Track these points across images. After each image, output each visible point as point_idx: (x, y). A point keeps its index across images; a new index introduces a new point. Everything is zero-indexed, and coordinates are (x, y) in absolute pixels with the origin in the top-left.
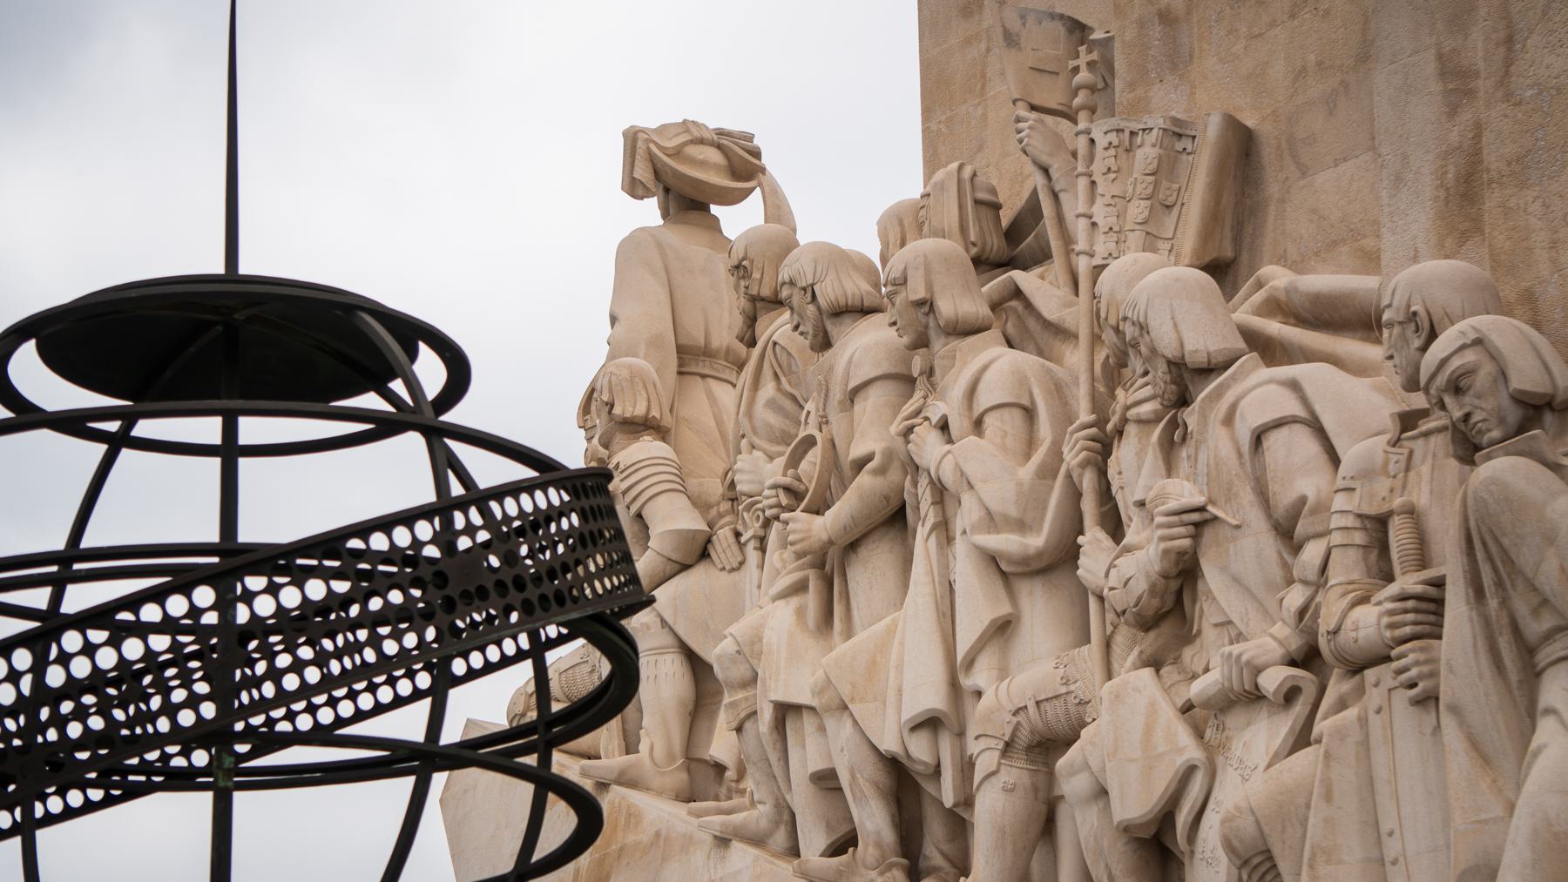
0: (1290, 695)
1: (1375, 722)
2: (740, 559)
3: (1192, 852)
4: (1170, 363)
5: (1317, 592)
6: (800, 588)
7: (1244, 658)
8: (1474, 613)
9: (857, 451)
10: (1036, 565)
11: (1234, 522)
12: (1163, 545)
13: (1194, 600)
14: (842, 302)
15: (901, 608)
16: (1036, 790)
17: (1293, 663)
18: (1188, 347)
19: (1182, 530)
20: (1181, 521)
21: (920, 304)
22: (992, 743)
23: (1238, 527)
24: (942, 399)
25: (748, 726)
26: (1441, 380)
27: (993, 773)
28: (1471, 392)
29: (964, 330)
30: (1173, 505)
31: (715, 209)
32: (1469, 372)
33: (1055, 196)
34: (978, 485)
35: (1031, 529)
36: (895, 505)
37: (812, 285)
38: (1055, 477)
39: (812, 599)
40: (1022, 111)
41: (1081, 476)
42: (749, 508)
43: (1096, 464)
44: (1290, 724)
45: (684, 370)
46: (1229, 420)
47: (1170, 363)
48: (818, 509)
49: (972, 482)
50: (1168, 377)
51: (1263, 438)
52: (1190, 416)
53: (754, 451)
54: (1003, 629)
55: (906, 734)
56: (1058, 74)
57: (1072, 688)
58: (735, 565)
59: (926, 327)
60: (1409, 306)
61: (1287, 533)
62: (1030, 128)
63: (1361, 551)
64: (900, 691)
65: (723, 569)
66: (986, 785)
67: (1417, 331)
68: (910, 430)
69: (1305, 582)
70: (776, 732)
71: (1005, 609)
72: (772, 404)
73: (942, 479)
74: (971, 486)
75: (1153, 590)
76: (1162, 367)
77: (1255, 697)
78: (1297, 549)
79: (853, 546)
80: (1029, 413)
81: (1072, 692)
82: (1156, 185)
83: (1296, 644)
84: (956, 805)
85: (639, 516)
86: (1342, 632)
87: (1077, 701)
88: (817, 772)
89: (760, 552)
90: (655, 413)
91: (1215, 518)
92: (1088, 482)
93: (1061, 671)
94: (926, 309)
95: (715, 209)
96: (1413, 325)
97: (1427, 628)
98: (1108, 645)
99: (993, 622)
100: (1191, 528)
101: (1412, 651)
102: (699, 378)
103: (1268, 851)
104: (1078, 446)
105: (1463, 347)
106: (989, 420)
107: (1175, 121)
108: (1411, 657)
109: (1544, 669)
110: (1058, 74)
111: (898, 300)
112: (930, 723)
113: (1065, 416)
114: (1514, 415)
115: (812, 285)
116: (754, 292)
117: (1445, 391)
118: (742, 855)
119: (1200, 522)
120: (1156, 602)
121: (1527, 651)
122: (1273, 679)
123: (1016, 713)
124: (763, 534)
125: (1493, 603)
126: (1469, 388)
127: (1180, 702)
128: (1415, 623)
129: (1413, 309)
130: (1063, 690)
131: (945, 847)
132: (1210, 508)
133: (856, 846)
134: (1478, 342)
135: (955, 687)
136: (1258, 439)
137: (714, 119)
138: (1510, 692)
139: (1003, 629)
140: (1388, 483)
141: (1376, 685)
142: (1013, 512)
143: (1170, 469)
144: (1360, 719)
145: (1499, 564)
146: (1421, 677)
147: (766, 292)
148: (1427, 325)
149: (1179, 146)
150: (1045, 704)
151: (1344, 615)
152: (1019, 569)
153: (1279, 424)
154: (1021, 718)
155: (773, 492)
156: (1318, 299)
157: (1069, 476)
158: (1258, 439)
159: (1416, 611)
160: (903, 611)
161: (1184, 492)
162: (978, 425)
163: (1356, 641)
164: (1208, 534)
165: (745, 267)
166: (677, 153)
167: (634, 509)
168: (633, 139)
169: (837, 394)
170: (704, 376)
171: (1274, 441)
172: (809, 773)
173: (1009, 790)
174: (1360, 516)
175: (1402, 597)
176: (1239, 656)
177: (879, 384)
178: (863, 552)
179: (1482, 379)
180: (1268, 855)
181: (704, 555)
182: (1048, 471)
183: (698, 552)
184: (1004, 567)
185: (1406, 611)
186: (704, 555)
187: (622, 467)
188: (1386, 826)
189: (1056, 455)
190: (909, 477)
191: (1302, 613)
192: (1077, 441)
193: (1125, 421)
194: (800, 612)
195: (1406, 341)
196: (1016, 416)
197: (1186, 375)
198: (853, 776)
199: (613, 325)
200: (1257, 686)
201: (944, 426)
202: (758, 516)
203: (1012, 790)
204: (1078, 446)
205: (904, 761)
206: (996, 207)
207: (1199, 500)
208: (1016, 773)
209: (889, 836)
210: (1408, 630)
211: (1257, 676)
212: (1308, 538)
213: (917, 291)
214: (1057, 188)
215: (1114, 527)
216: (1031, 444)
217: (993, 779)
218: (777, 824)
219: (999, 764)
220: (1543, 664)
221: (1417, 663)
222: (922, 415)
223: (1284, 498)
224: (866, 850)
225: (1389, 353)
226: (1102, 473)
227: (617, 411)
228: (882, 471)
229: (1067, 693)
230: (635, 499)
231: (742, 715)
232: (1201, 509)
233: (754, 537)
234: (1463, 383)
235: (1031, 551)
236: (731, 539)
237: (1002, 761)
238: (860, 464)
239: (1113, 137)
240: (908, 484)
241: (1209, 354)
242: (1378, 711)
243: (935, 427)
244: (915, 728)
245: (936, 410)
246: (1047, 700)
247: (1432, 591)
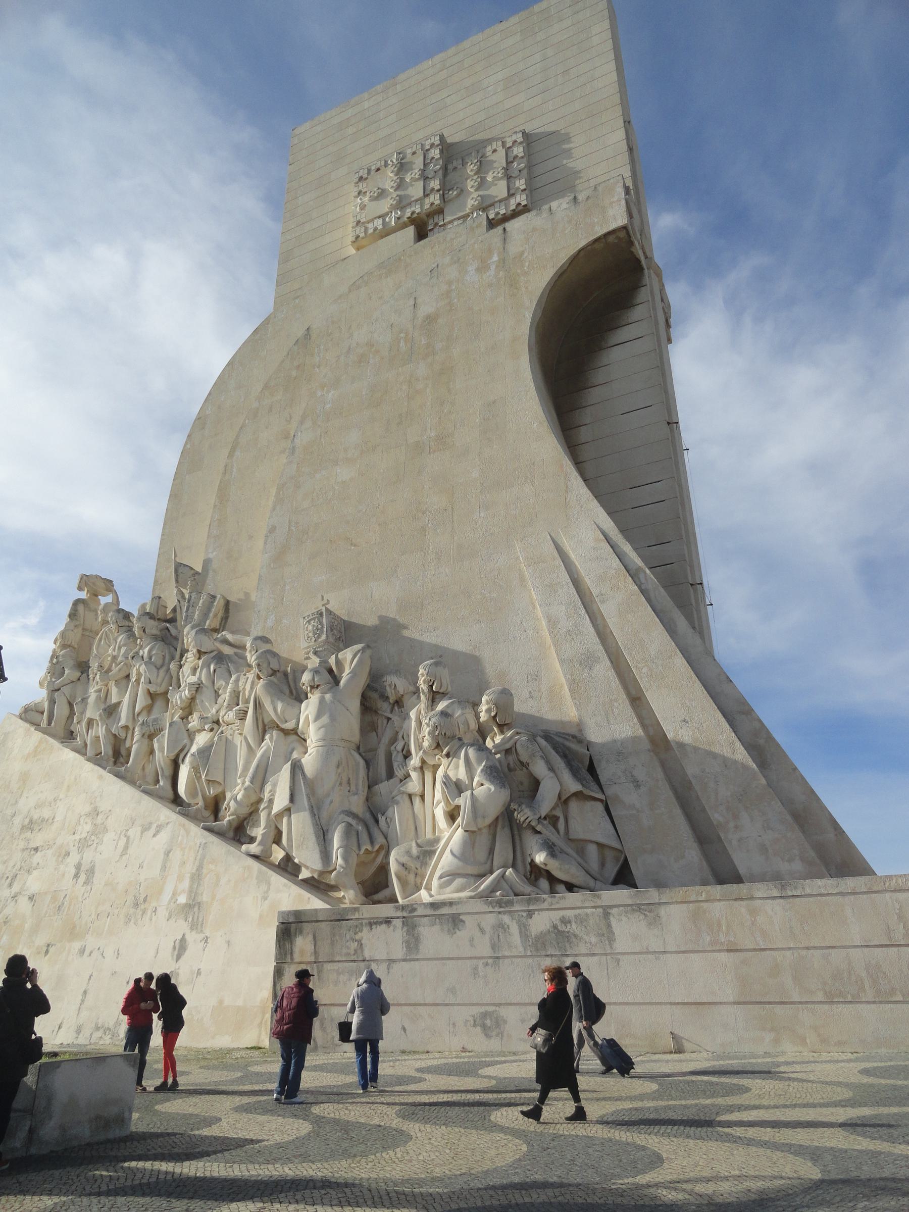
83: (215, 719)
112: (126, 728)
121: (264, 725)
161: (194, 679)
226: (178, 673)
247: (246, 709)
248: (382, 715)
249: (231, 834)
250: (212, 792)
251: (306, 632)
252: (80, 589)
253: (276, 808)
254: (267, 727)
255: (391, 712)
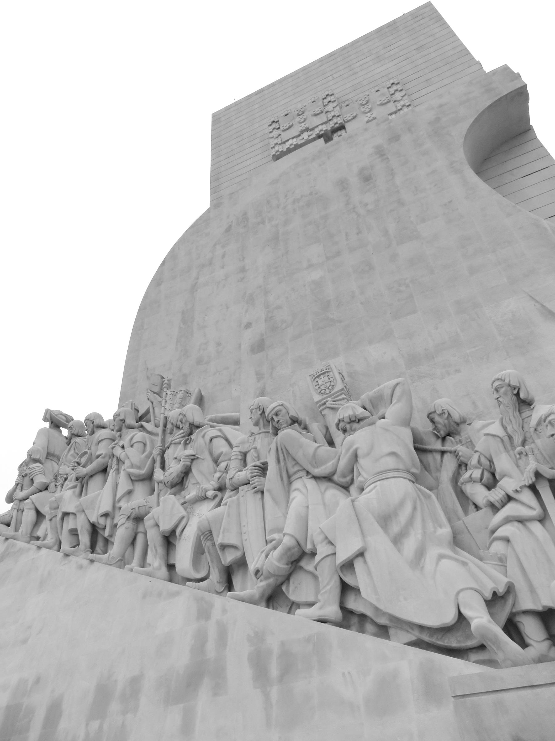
0: (215, 497)
1: (241, 499)
2: (55, 490)
3: (180, 539)
4: (190, 424)
5: (223, 474)
6: (75, 487)
7: (204, 488)
8: (277, 466)
9: (98, 453)
10: (141, 478)
11: (203, 458)
12: (183, 463)
13: (186, 480)
14: (100, 424)
15: (102, 489)
16: (133, 529)
17: (215, 490)
18: (195, 420)
19: (189, 460)
20: (189, 458)
21: (122, 420)
22: (124, 516)
23: (203, 459)
24: (124, 441)
25: (54, 519)
26: (273, 412)
27: (124, 524)
28: (281, 415)
29: (130, 427)
30: (185, 454)
31: (61, 428)
32: (280, 411)
33: (154, 408)
34: (131, 458)
35: (142, 469)
36: (104, 467)
37: (93, 420)
38: (149, 458)
39: (78, 490)
40: (149, 391)
41: (157, 457)
42: (61, 477)
43: (161, 455)
44: (214, 504)
45: (47, 457)
46: (203, 437)
47: (190, 424)
48: (84, 466)
49: (129, 457)
50: (189, 427)
51: (212, 440)
52: (193, 437)
53: (65, 466)
54: (129, 493)
55: (99, 517)
56: (157, 386)
57: (148, 504)
58: (54, 491)
59: (122, 426)
60: (258, 405)
61: (216, 462)
62: (151, 394)
63: (239, 460)
64: (99, 507)
65: (50, 492)
66: (121, 527)
67: (260, 410)
68: (114, 447)
69: (220, 471)
70: (61, 520)
71: (131, 487)
72: (72, 455)
73: (121, 458)
74: (128, 458)
75: (177, 476)
76: (188, 424)
77: (205, 498)
78: (218, 466)
79: (91, 476)
80: (145, 445)
81: (147, 505)
82: (182, 401)
83: (216, 486)
84: (108, 536)
85: (32, 479)
86: (234, 479)
87: (149, 507)
88: (71, 529)
89: (61, 488)
90: (41, 458)
91: (198, 458)
92: (158, 459)
93: (146, 500)
94: (123, 421)
95: (61, 428)
96: (259, 409)
97: (260, 474)
98: (159, 495)
99: (128, 490)
100: (191, 460)
101: (256, 478)
102: (50, 460)
103: (211, 530)
104: (157, 450)
105: (279, 405)
106: (135, 445)
107: (187, 390)
108: (256, 480)
109: (292, 482)
110: (157, 386)
111: (116, 420)
112: (106, 515)
113: (153, 447)
114: (290, 422)
115: (93, 420)
116: (73, 432)
117: (274, 415)
118: (44, 551)
119: (193, 458)
120: (177, 479)
121: (289, 477)
122: (210, 493)
123: (132, 509)
124: (63, 483)
125: (282, 463)
126: (280, 414)
127: (182, 501)
128: (257, 473)
129: (259, 405)
130: (146, 504)
131: (102, 548)
132: (196, 455)
133: (79, 546)
134: (282, 405)
135: (114, 507)
136: (211, 440)
137: (65, 412)
138: (284, 487)
139: (129, 493)
140: (248, 444)
141: (242, 490)
142: (138, 464)
143: (185, 448)
144: (237, 499)
145: (285, 454)
146: (258, 485)
147: (76, 433)
148: (262, 409)
149: (187, 395)
150: (140, 508)
151: (235, 474)
152: (137, 479)
153: (217, 437)
154: (133, 511)
155: (73, 463)
156: (223, 418)
157: (153, 458)
158: (211, 440)
159: (258, 469)
160: (103, 490)
161: (190, 451)
162: (132, 446)
163: (239, 479)
164: (195, 462)
165: (72, 427)
166: (56, 415)
167: (31, 477)
168: (47, 411)
169: (95, 441)
170: (51, 460)
171: (215, 441)
172: (69, 529)
173: (127, 528)
174: (240, 452)
175: (255, 466)
176: (202, 487)
177: (106, 440)
178: (94, 478)
179: (284, 411)
180: (210, 531)
181: (46, 489)
182: (148, 457)
183: (45, 487)
184: (132, 478)
185: (255, 469)
186: (46, 489)
187: (30, 468)
188: (243, 524)
189: (151, 453)
190: (111, 459)
191: (219, 478)
192: (157, 449)
193: (171, 444)
194: (74, 492)
195: (257, 413)
196: (141, 445)
197: (193, 428)
198: (82, 528)
199: (33, 445)
200: (205, 496)
201: (123, 447)
202: (63, 480)
203: (128, 528)
204: (157, 450)
205: (97, 525)
206: (138, 411)
207: (194, 453)
208: (130, 524)
209: (88, 543)
210: (256, 474)
211: (206, 492)
212: (222, 462)
213: (122, 417)
214: (154, 407)
215: (163, 468)
216: (144, 451)
217: (123, 526)
218: (55, 544)
219: (125, 522)
220: (293, 480)
221: (257, 482)
222: (118, 444)
223: (216, 452)
224: (82, 546)
225: (251, 417)
227: (32, 457)
228: (104, 457)
229: (146, 505)
230: (32, 475)
231: (53, 516)
232: (194, 456)
233: (61, 484)
234: (278, 413)
235: (141, 474)
236: (54, 485)
237: (127, 521)
238: (98, 457)
239: (172, 393)
240: (110, 460)
241: (200, 423)
242: (243, 496)
243: (120, 447)
244: (102, 516)
245: (121, 444)
246: (141, 506)
248: (431, 451)
249: (264, 603)
250: (229, 557)
251: (317, 387)
252: (45, 420)
253: (342, 557)
254: (293, 478)
255: (443, 445)
